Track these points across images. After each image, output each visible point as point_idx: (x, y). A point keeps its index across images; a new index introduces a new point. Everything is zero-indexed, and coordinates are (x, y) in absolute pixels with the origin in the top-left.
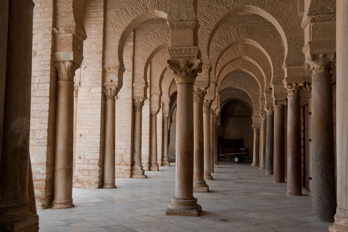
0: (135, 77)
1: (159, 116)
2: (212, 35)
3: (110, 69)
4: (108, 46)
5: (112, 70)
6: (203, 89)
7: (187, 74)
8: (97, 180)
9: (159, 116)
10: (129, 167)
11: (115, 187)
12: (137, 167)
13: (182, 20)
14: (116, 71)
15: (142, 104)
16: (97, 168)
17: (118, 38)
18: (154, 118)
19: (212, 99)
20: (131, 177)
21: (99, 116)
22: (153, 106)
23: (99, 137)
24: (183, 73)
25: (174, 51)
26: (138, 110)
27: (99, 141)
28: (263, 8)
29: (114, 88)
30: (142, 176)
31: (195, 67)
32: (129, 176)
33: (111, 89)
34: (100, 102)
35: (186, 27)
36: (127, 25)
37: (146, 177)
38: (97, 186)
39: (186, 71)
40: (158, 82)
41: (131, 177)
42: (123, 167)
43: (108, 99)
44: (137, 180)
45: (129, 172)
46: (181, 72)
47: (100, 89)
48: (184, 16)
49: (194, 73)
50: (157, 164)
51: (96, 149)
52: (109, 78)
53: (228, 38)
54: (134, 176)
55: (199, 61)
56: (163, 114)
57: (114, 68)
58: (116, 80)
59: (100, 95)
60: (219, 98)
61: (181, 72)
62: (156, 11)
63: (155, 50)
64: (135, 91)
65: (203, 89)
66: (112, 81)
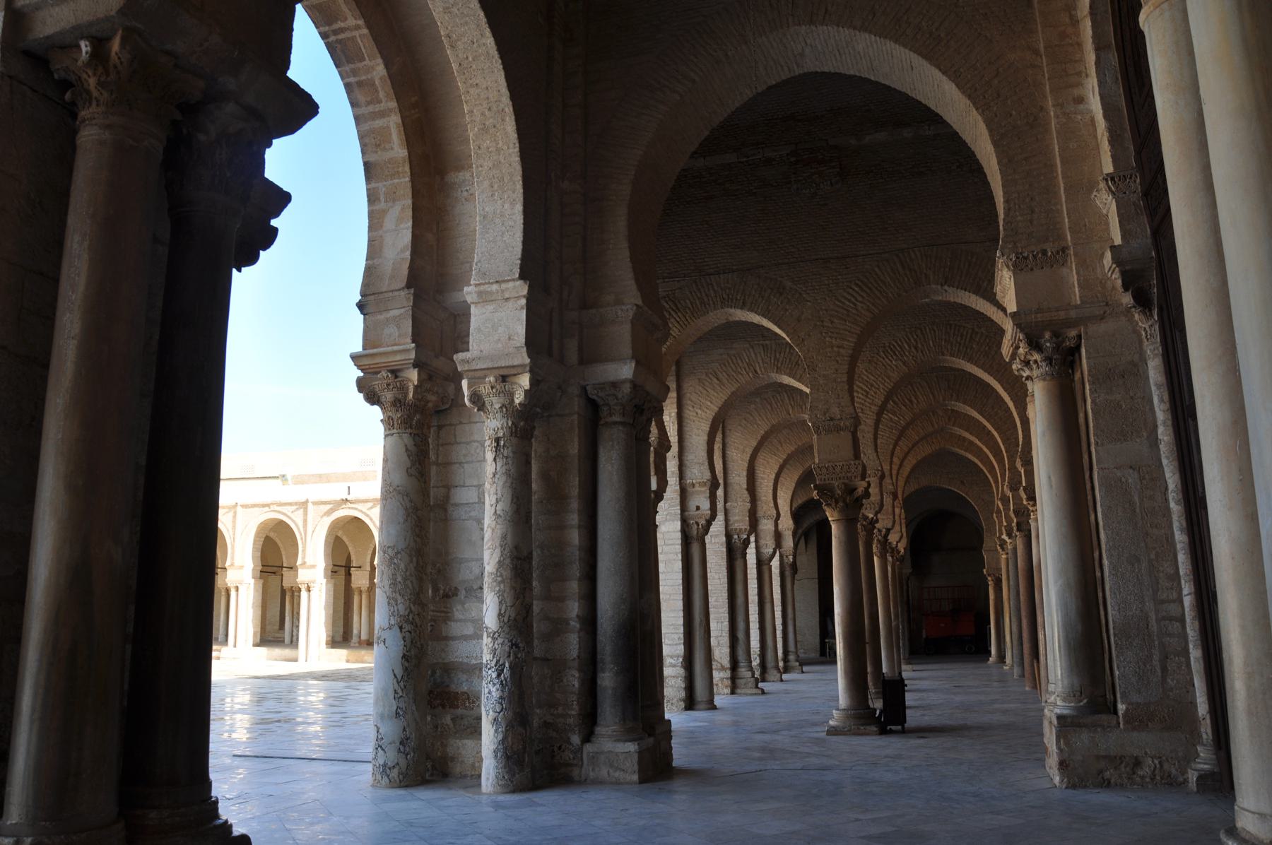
0: (730, 489)
1: (775, 563)
2: (879, 414)
3: (693, 485)
4: (687, 444)
5: (697, 488)
6: (871, 516)
7: (847, 505)
8: (683, 694)
9: (775, 563)
10: (728, 674)
11: (715, 708)
12: (743, 672)
13: (832, 419)
14: (705, 491)
15: (746, 543)
16: (681, 671)
17: (706, 427)
18: (765, 568)
19: (889, 526)
20: (733, 693)
21: (680, 576)
22: (762, 542)
23: (681, 614)
24: (841, 504)
25: (824, 470)
26: (738, 555)
27: (681, 621)
28: (970, 360)
29: (702, 522)
30: (755, 691)
31: (860, 490)
32: (727, 691)
33: (697, 523)
34: (679, 548)
35: (838, 429)
36: (720, 403)
37: (763, 692)
38: (682, 705)
39: (844, 501)
40: (771, 492)
41: (733, 693)
42: (722, 674)
43: (691, 540)
44: (745, 699)
45: (728, 682)
46: (837, 503)
47: (678, 525)
48: (835, 411)
49: (858, 503)
50: (777, 667)
51: (676, 636)
52: (692, 505)
53: (911, 401)
54: (739, 691)
55: (864, 484)
56: (781, 556)
57: (702, 484)
58: (705, 505)
59: (679, 535)
60: (903, 516)
61: (837, 503)
62: (773, 375)
63: (766, 432)
64: (732, 519)
65: (871, 516)
66: (698, 508)
